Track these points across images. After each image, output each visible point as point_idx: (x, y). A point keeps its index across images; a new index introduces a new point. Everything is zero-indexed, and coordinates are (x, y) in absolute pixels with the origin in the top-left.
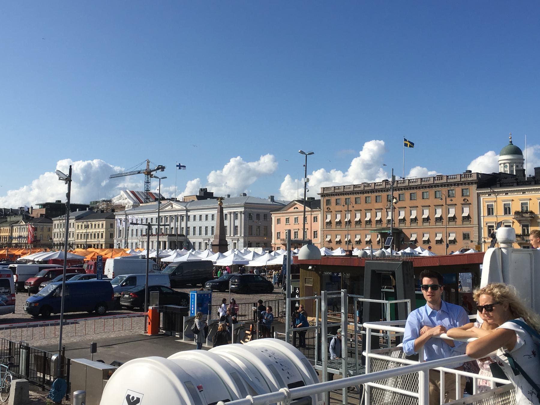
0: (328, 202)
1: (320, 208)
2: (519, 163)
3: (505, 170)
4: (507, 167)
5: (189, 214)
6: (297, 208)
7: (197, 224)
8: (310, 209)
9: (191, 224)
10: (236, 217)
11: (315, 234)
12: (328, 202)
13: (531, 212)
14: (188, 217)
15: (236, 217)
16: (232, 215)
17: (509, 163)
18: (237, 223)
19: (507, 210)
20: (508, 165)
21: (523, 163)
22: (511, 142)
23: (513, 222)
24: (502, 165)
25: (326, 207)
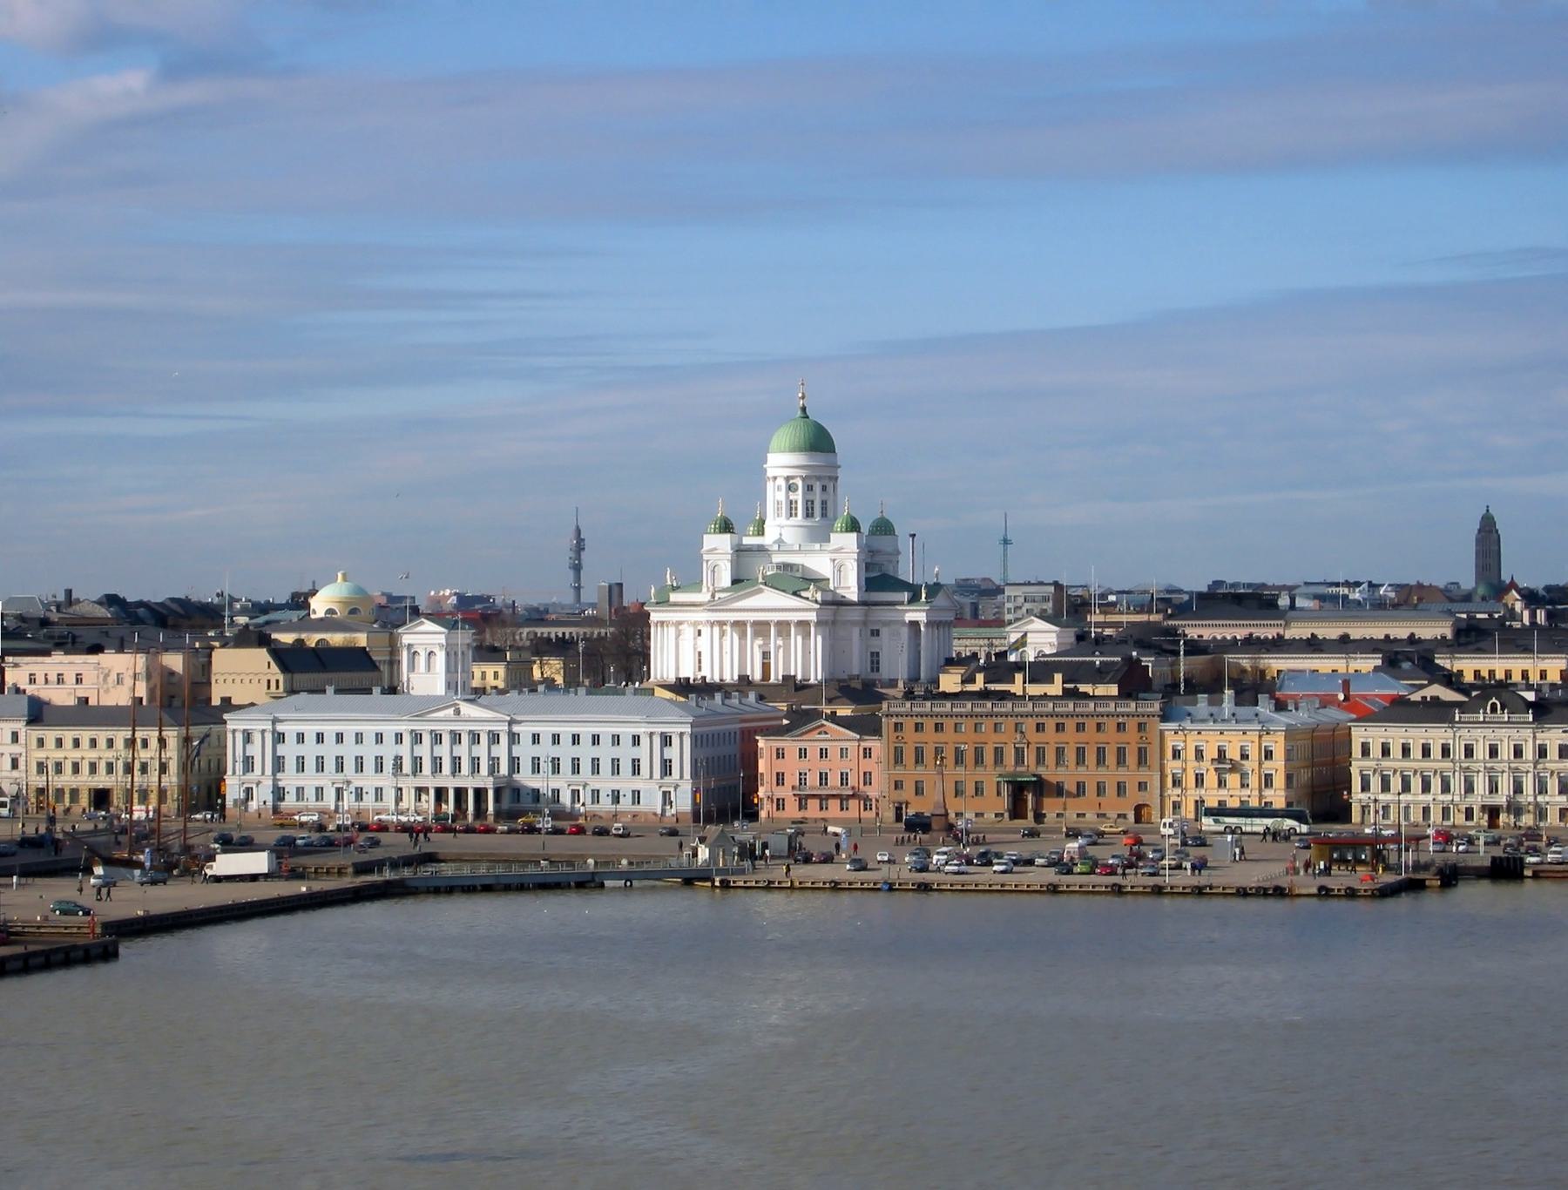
0: (898, 727)
1: (881, 736)
2: (830, 478)
3: (791, 498)
4: (796, 490)
5: (516, 729)
6: (826, 733)
7: (546, 750)
8: (858, 737)
9: (525, 751)
10: (666, 740)
11: (867, 778)
12: (898, 727)
13: (1231, 760)
14: (514, 738)
15: (666, 740)
16: (657, 741)
17: (804, 479)
18: (672, 753)
19: (1199, 754)
20: (799, 483)
21: (837, 478)
22: (804, 409)
23: (1208, 770)
24: (781, 482)
25: (893, 735)
